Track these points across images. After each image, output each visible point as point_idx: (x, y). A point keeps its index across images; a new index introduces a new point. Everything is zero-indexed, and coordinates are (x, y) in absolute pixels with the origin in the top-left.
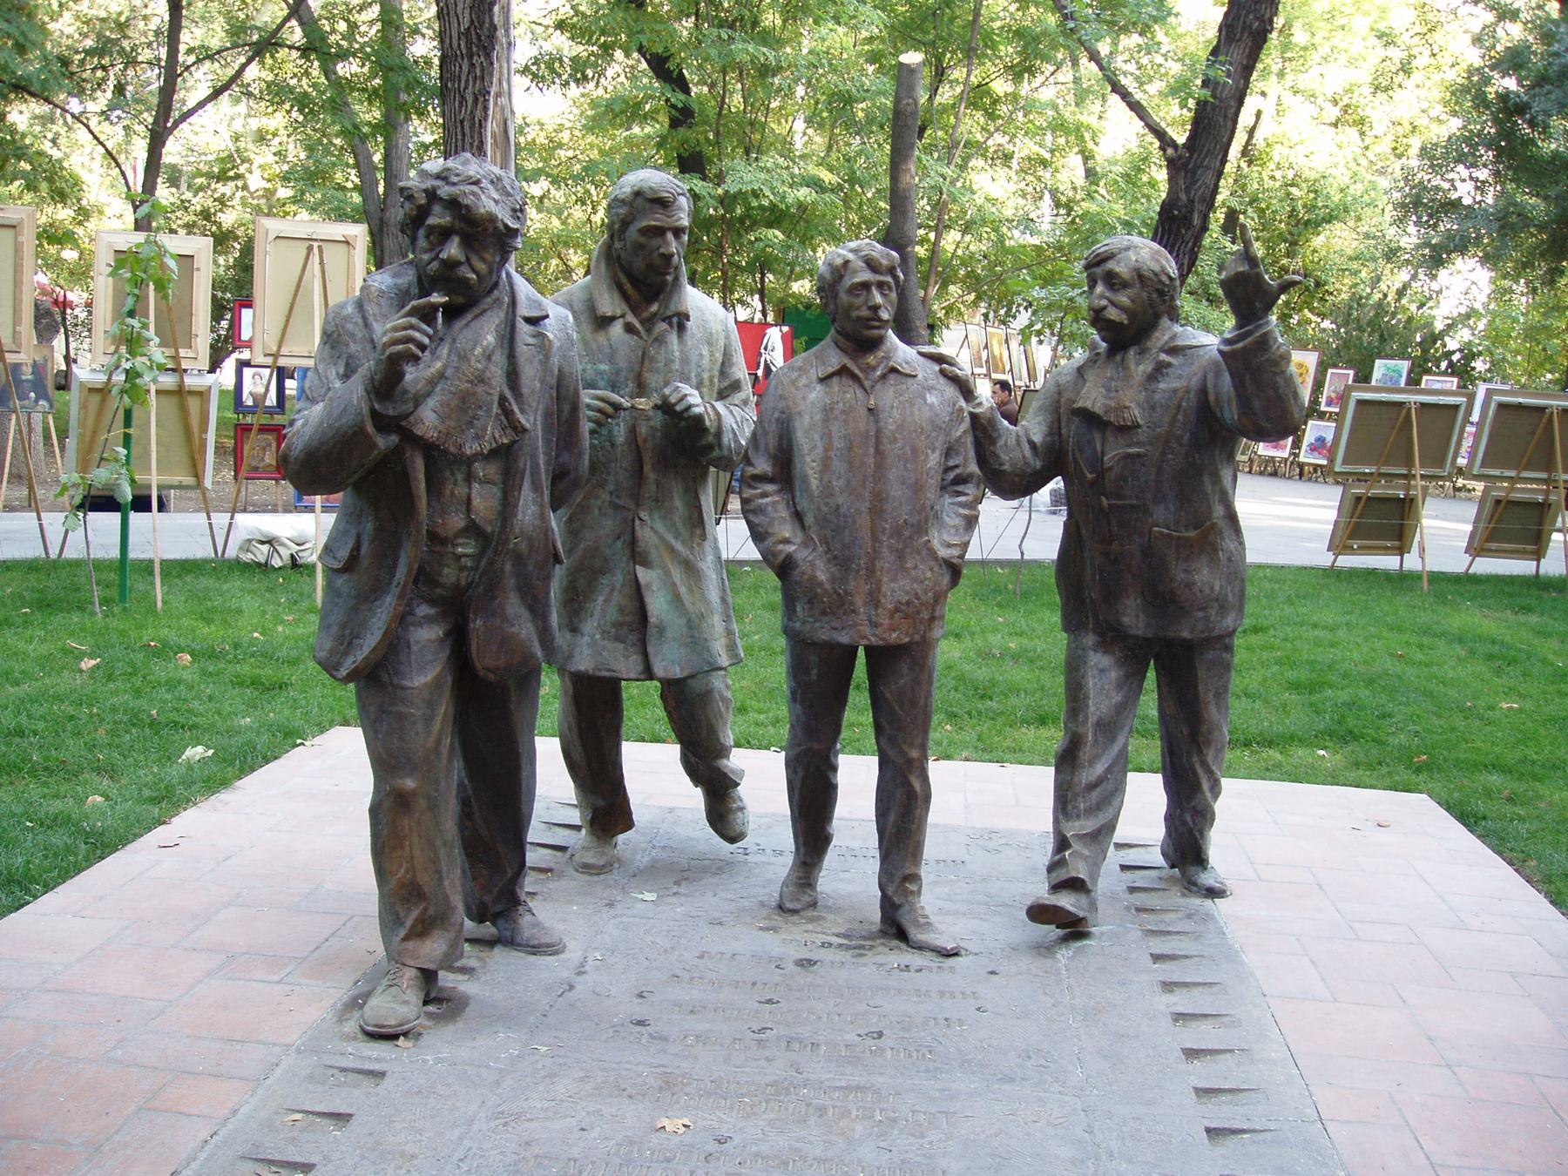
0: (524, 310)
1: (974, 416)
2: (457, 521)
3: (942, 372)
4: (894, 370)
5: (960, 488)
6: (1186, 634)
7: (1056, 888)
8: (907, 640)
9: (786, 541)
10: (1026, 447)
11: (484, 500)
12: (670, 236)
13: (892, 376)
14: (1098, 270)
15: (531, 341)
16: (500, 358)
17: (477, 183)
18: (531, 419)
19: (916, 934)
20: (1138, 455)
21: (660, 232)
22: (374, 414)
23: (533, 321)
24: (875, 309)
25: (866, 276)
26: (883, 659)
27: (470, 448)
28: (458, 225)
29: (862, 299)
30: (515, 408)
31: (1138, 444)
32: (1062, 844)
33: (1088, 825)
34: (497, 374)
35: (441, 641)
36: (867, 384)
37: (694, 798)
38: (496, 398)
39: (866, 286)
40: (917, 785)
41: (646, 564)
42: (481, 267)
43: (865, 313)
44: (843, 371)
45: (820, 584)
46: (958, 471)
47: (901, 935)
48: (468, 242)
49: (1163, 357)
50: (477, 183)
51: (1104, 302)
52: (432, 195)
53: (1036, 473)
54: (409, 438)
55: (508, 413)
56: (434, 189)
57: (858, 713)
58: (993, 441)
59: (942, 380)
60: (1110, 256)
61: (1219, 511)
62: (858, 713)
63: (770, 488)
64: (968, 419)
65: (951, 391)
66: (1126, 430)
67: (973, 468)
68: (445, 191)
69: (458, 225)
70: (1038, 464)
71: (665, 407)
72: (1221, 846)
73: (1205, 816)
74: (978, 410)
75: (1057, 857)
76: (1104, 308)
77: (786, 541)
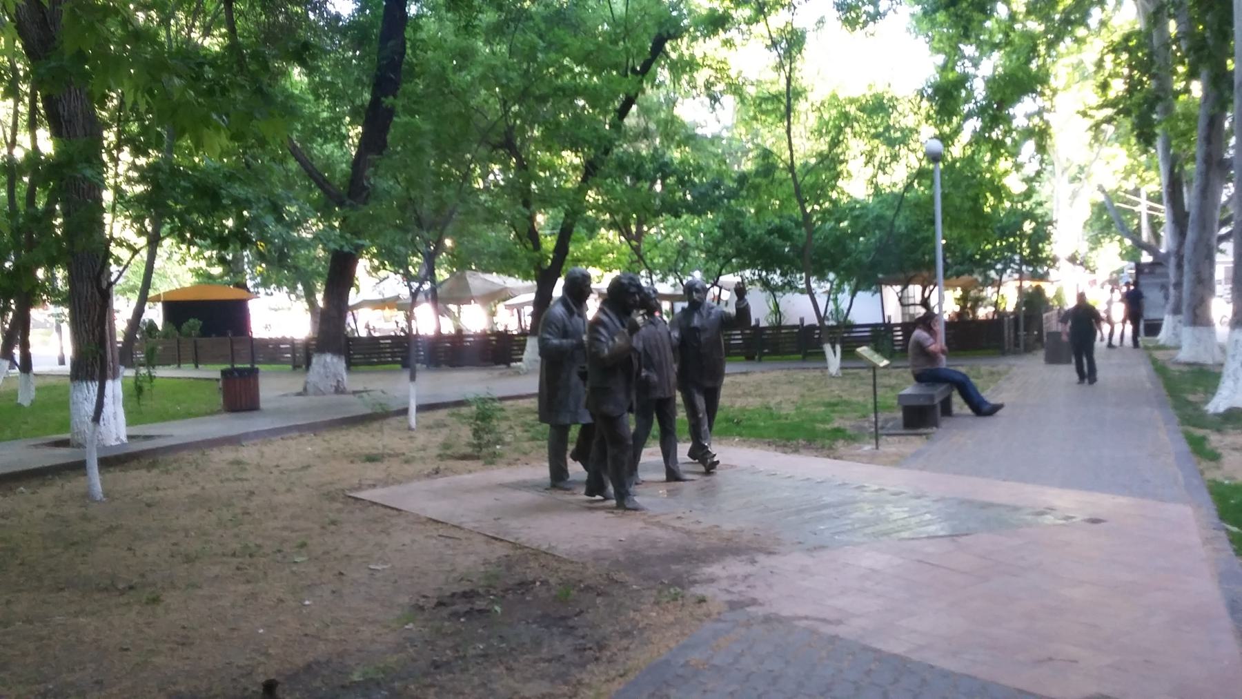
47: (678, 479)
52: (630, 284)
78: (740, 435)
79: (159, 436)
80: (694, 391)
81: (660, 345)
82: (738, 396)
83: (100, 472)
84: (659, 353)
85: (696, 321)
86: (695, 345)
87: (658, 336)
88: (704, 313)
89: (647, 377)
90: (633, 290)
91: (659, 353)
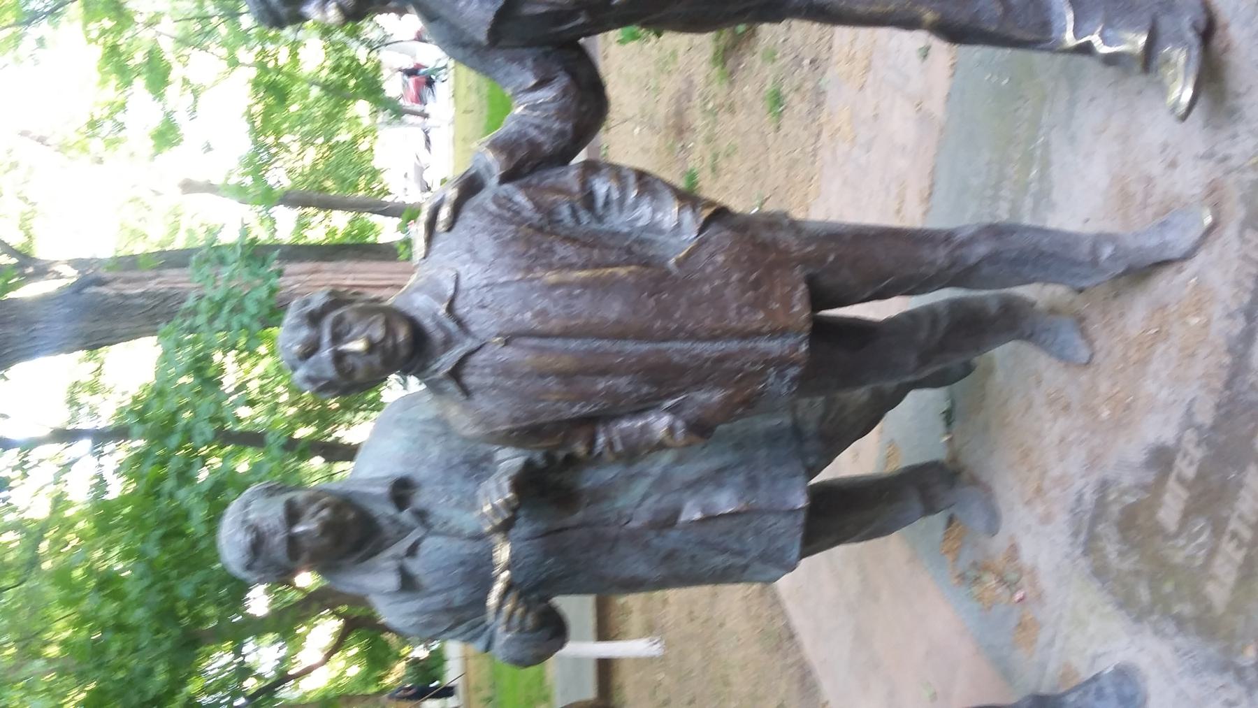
1: (505, 179)
3: (450, 227)
4: (450, 309)
5: (600, 202)
8: (803, 287)
9: (671, 430)
10: (545, 95)
12: (299, 529)
25: (326, 353)
26: (820, 297)
36: (469, 344)
39: (339, 357)
40: (981, 249)
41: (677, 513)
43: (376, 359)
45: (729, 397)
46: (578, 205)
53: (573, 75)
58: (534, 145)
59: (459, 226)
63: (601, 439)
64: (508, 187)
70: (562, 80)
74: (497, 171)
81: (565, 363)
84: (604, 372)
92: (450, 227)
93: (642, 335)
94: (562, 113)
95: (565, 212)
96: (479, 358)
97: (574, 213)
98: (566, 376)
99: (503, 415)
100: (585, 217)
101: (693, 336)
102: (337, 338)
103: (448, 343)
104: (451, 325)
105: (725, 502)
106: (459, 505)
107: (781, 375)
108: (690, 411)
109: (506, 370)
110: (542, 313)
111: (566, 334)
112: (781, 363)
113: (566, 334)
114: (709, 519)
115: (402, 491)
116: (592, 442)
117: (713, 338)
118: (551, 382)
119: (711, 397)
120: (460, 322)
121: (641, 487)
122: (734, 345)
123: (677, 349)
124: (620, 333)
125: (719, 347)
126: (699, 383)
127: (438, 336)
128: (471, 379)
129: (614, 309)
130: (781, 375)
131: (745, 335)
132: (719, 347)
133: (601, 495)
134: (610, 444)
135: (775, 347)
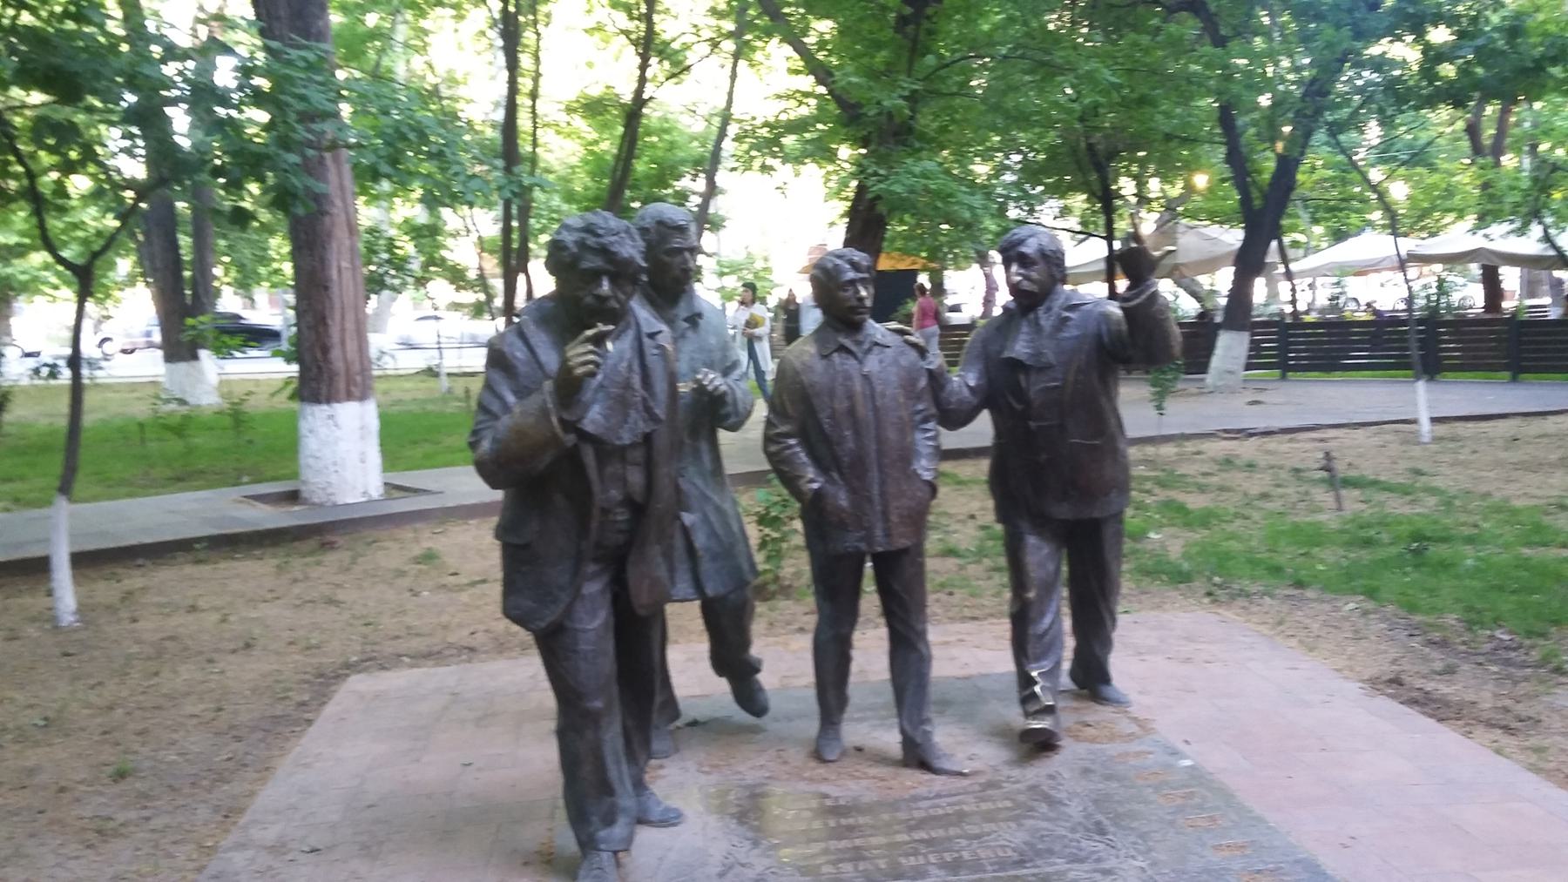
0: (646, 329)
1: (930, 372)
2: (615, 494)
4: (877, 344)
6: (1096, 514)
7: (1027, 715)
10: (966, 392)
11: (636, 477)
13: (876, 349)
14: (1012, 253)
15: (656, 351)
16: (636, 367)
17: (617, 234)
18: (660, 412)
19: (938, 764)
20: (1056, 387)
21: (680, 251)
22: (562, 421)
23: (652, 336)
24: (861, 299)
25: (851, 275)
27: (626, 438)
28: (609, 267)
29: (850, 293)
30: (652, 404)
31: (1055, 380)
32: (1026, 681)
33: (1046, 665)
34: (636, 381)
35: (602, 592)
36: (860, 355)
37: (722, 686)
38: (639, 399)
39: (852, 282)
41: (687, 510)
42: (622, 297)
43: (854, 303)
44: (842, 349)
45: (843, 510)
47: (924, 765)
48: (614, 280)
49: (1067, 314)
50: (617, 234)
51: (1019, 278)
52: (582, 244)
54: (584, 436)
55: (648, 410)
56: (583, 239)
57: (870, 601)
60: (1021, 242)
61: (1113, 421)
62: (870, 601)
63: (792, 442)
64: (926, 374)
65: (913, 354)
66: (1044, 368)
67: (933, 410)
68: (591, 241)
69: (609, 267)
70: (975, 401)
71: (700, 390)
72: (1121, 665)
73: (1107, 644)
74: (931, 367)
75: (1027, 692)
76: (1020, 282)
77: (812, 481)
78: (1371, 593)
79: (425, 492)
80: (1025, 525)
81: (863, 410)
82: (1536, 466)
83: (74, 577)
84: (857, 433)
85: (1020, 348)
86: (1018, 407)
87: (858, 386)
88: (1046, 322)
89: (817, 492)
90: (591, 262)
91: (857, 433)
92: (907, 342)
93: (880, 453)
94: (961, 402)
95: (920, 407)
96: (853, 362)
97: (920, 412)
98: (852, 412)
99: (816, 379)
100: (918, 417)
101: (883, 483)
102: (862, 280)
103: (859, 343)
104: (866, 346)
105: (700, 540)
106: (692, 359)
107: (861, 539)
108: (830, 489)
109: (848, 378)
110: (883, 395)
111: (876, 410)
112: (869, 539)
113: (876, 410)
114: (686, 532)
115: (694, 319)
116: (788, 435)
117: (883, 494)
118: (846, 404)
119: (843, 500)
120: (869, 351)
121: (699, 482)
122: (879, 508)
123: (874, 474)
124: (880, 440)
125: (876, 498)
126: (853, 491)
127: (860, 337)
128: (836, 357)
129: (892, 434)
130: (861, 539)
131: (885, 515)
132: (876, 498)
133: (696, 453)
134: (791, 447)
135: (879, 532)
